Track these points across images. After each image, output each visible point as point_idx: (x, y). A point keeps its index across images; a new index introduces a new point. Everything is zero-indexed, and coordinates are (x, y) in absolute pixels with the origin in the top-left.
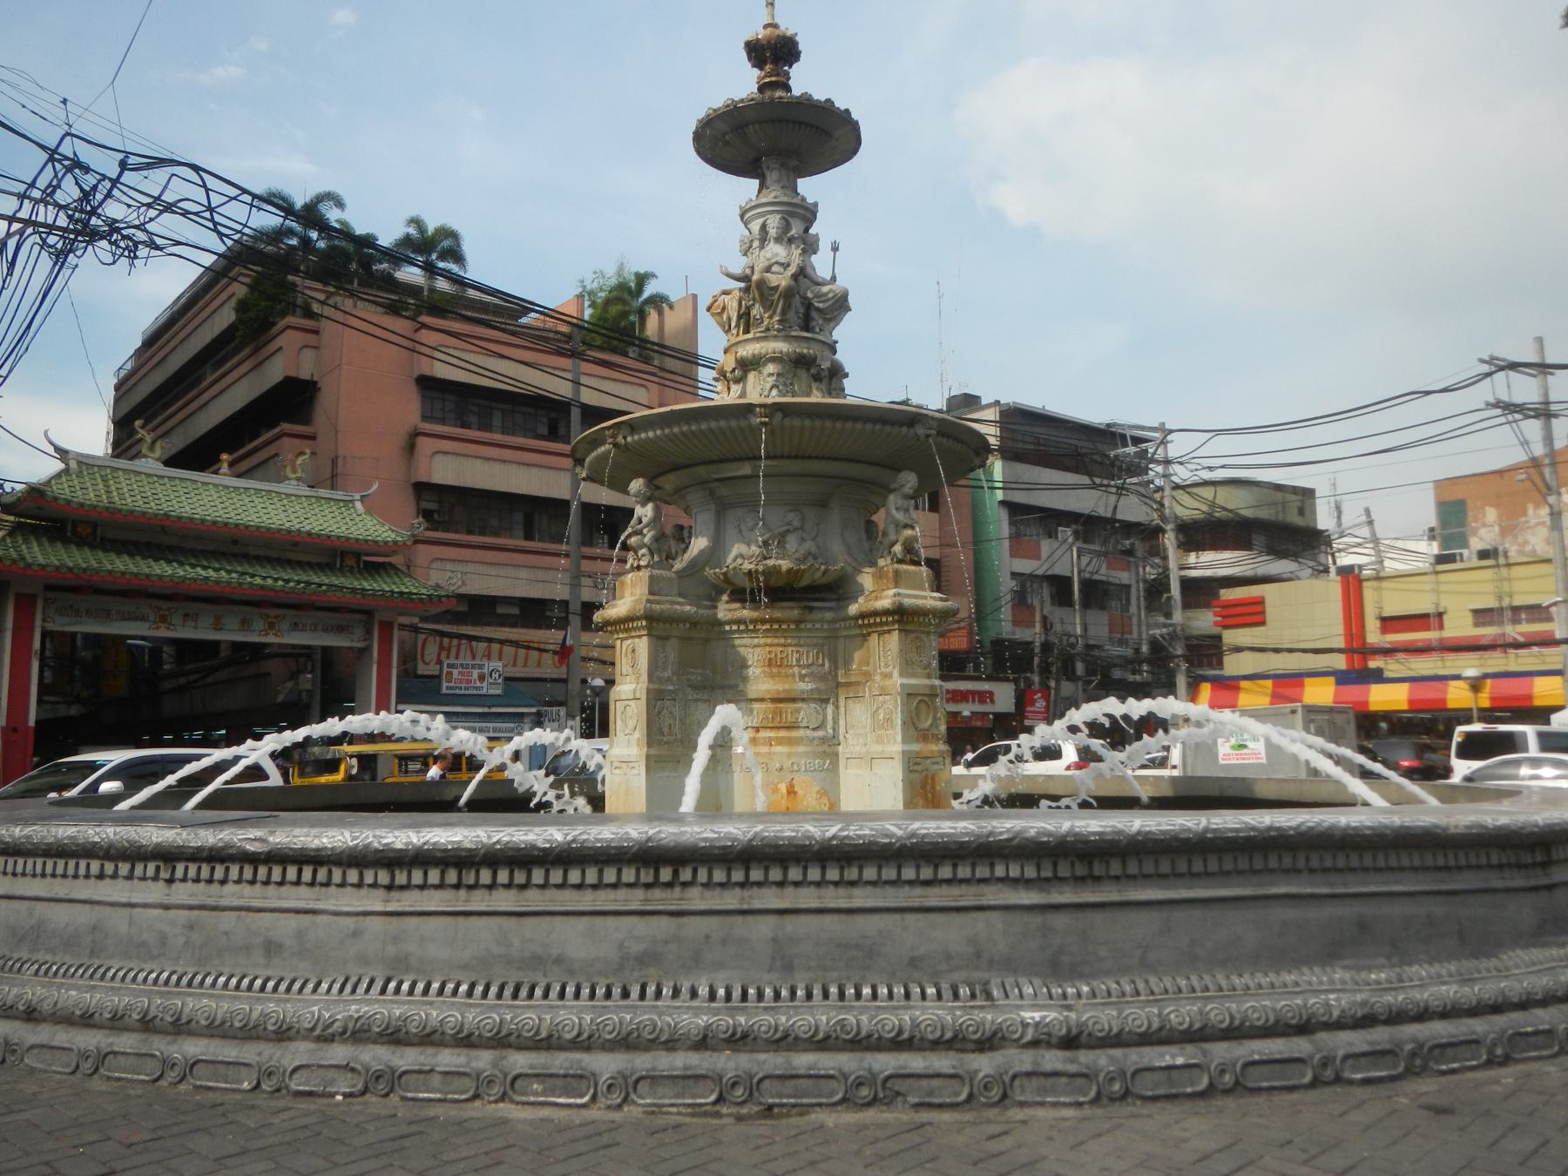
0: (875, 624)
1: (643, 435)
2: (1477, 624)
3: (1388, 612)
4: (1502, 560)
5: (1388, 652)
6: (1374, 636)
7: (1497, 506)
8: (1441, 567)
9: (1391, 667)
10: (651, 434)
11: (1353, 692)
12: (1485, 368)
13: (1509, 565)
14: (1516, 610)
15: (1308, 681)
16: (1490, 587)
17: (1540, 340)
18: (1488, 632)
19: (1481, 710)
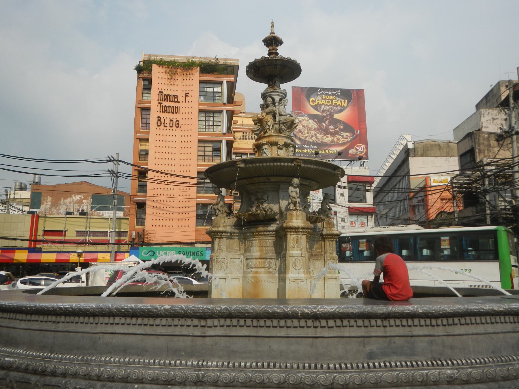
0: (329, 238)
1: (309, 166)
2: (77, 236)
3: (46, 229)
4: (89, 217)
5: (46, 242)
6: (40, 235)
7: (52, 196)
8: (68, 216)
9: (44, 247)
10: (312, 166)
11: (34, 256)
12: (108, 159)
13: (90, 218)
14: (90, 231)
15: (17, 251)
16: (85, 224)
17: (118, 154)
18: (82, 238)
19: (80, 263)
